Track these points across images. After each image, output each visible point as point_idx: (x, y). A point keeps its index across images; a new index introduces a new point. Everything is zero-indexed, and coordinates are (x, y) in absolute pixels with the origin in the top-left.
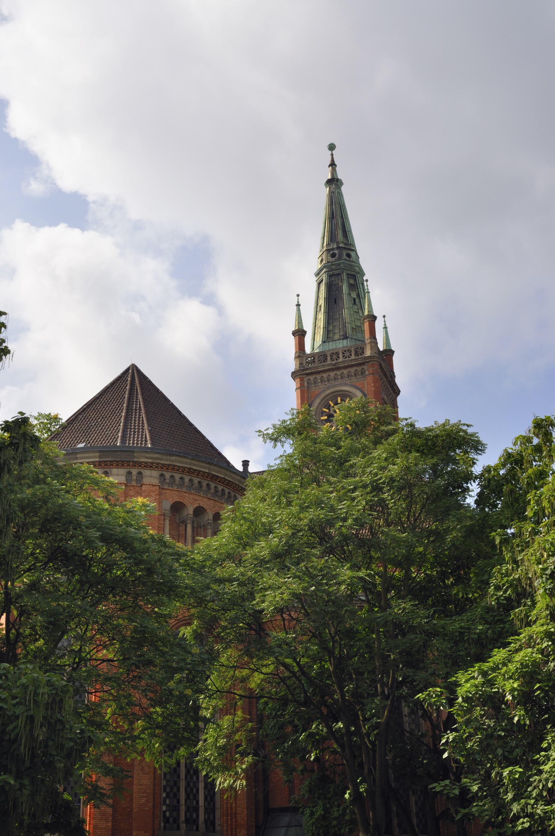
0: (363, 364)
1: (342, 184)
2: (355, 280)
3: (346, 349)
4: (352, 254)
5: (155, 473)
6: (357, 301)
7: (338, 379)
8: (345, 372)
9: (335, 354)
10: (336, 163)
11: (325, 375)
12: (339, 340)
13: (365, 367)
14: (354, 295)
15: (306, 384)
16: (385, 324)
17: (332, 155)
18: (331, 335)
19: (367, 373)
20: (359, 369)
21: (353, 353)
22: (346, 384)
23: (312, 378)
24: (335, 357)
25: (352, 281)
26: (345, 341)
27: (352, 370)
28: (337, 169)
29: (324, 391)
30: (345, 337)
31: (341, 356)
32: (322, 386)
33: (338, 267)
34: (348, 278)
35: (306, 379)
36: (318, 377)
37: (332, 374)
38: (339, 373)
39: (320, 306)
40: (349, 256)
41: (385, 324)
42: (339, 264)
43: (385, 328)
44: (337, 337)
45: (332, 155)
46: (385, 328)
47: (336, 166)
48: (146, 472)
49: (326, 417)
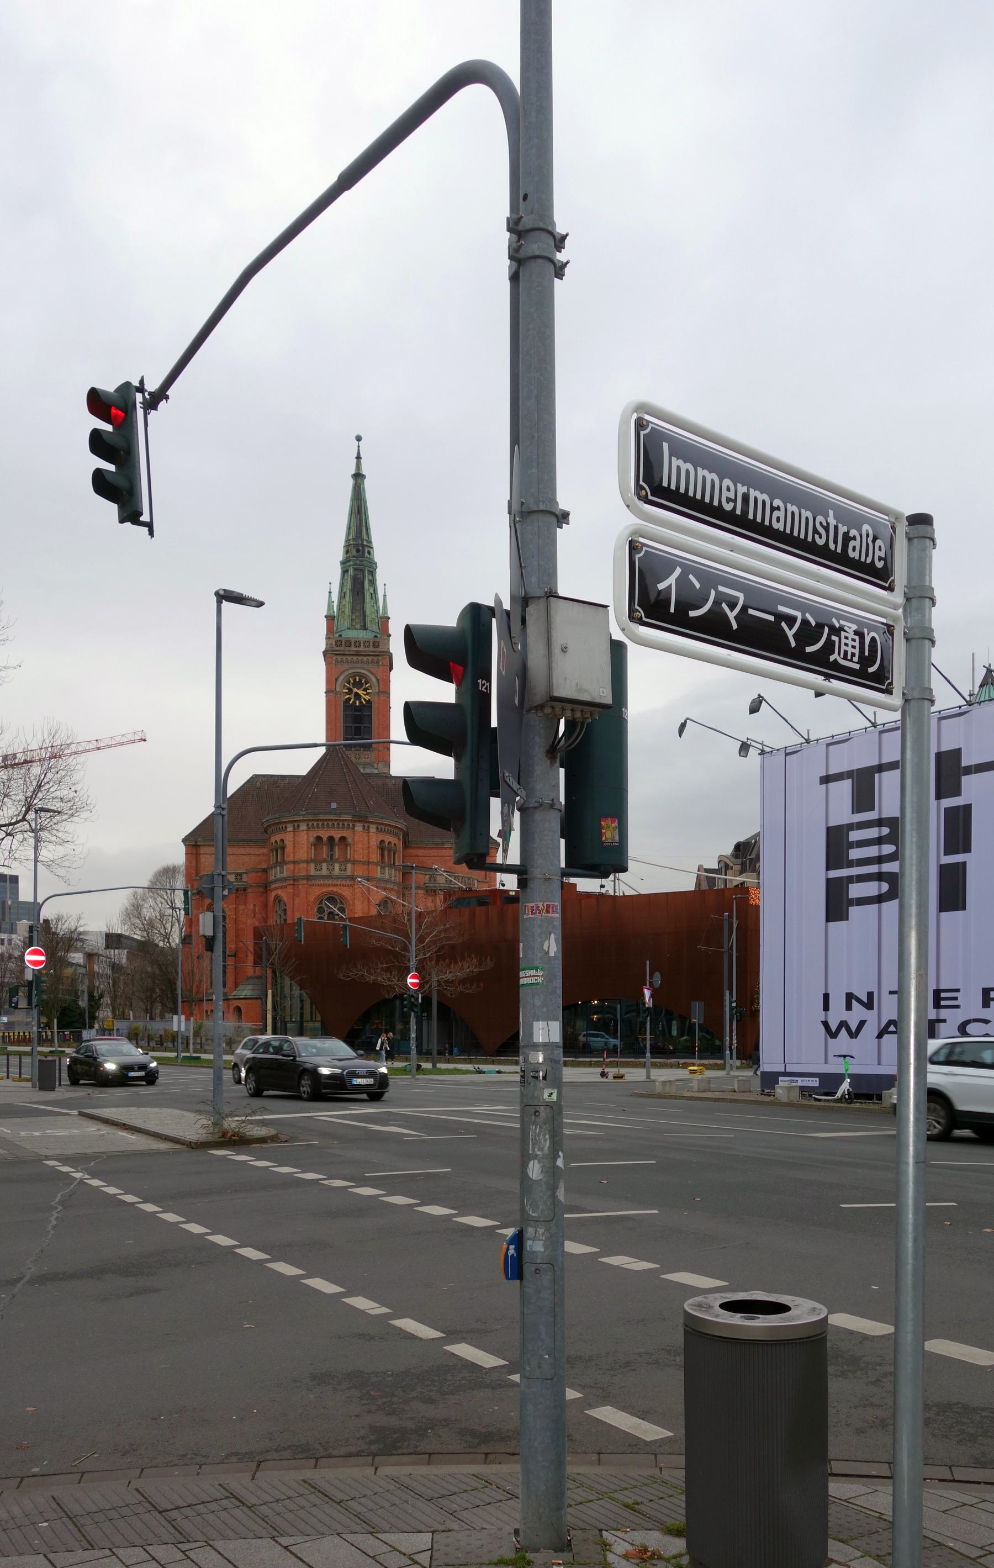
0: (378, 655)
1: (365, 478)
2: (373, 576)
3: (367, 640)
4: (371, 551)
5: (375, 826)
6: (373, 595)
7: (358, 663)
8: (365, 659)
9: (357, 643)
10: (361, 456)
11: (349, 658)
12: (360, 629)
13: (380, 658)
14: (372, 591)
15: (334, 662)
16: (385, 592)
17: (359, 446)
18: (354, 623)
19: (380, 663)
20: (375, 658)
21: (371, 644)
22: (364, 669)
23: (339, 658)
24: (357, 644)
25: (370, 577)
26: (365, 631)
27: (370, 658)
28: (362, 461)
29: (347, 670)
30: (364, 628)
31: (362, 644)
32: (346, 666)
33: (361, 563)
34: (368, 574)
35: (334, 658)
36: (344, 658)
37: (355, 658)
38: (360, 658)
39: (345, 593)
40: (369, 553)
41: (385, 592)
42: (362, 561)
43: (385, 596)
44: (358, 626)
45: (359, 446)
46: (385, 596)
47: (361, 458)
48: (371, 826)
49: (347, 691)
